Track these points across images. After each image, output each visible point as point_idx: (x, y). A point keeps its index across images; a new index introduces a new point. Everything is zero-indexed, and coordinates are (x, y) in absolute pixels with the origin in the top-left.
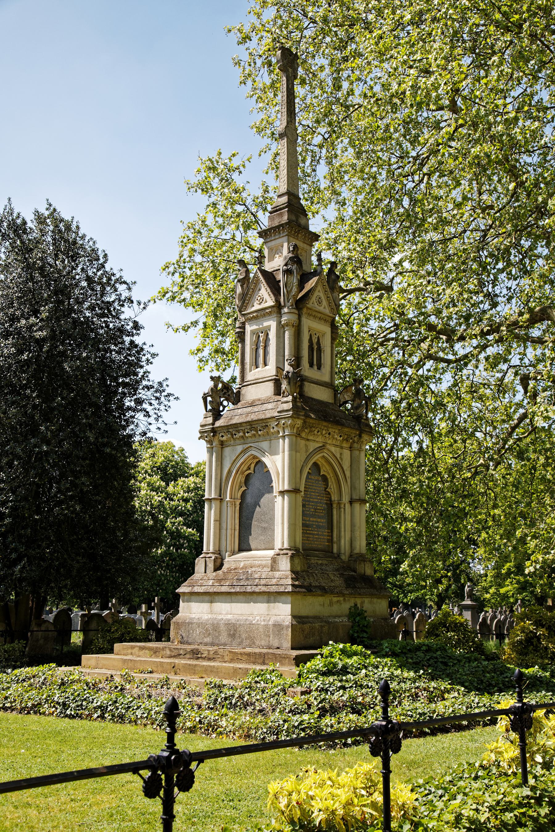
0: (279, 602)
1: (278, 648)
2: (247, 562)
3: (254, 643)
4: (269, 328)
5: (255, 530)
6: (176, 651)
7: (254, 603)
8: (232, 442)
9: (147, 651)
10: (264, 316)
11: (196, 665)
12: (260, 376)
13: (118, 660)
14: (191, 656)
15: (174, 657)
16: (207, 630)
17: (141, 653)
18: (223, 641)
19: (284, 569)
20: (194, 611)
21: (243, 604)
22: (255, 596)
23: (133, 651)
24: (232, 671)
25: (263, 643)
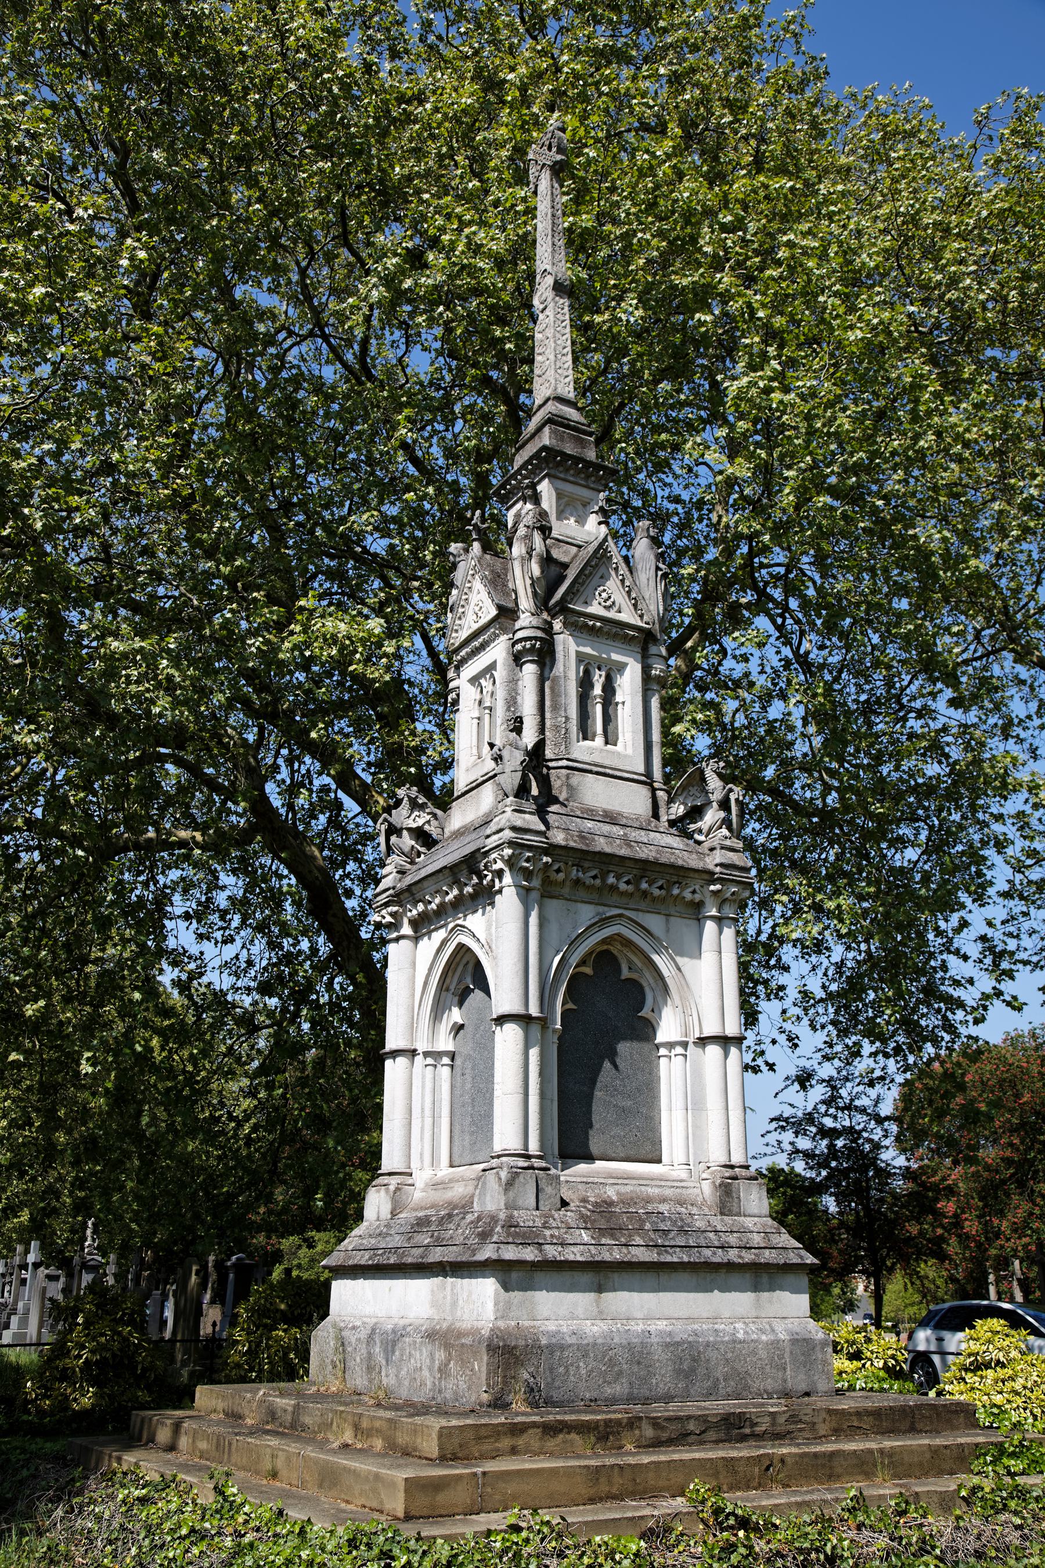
0: (782, 1289)
1: (807, 1394)
2: (623, 1189)
3: (746, 1387)
4: (621, 667)
5: (599, 1114)
6: (673, 1427)
7: (723, 1290)
8: (566, 891)
9: (573, 1436)
10: (615, 637)
11: (833, 1454)
12: (607, 763)
13: (569, 1472)
14: (722, 1435)
15: (671, 1442)
16: (612, 1363)
17: (551, 1444)
18: (662, 1389)
19: (756, 1211)
20: (546, 1314)
21: (692, 1295)
22: (722, 1276)
23: (521, 1442)
24: (928, 1456)
25: (770, 1384)
